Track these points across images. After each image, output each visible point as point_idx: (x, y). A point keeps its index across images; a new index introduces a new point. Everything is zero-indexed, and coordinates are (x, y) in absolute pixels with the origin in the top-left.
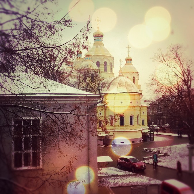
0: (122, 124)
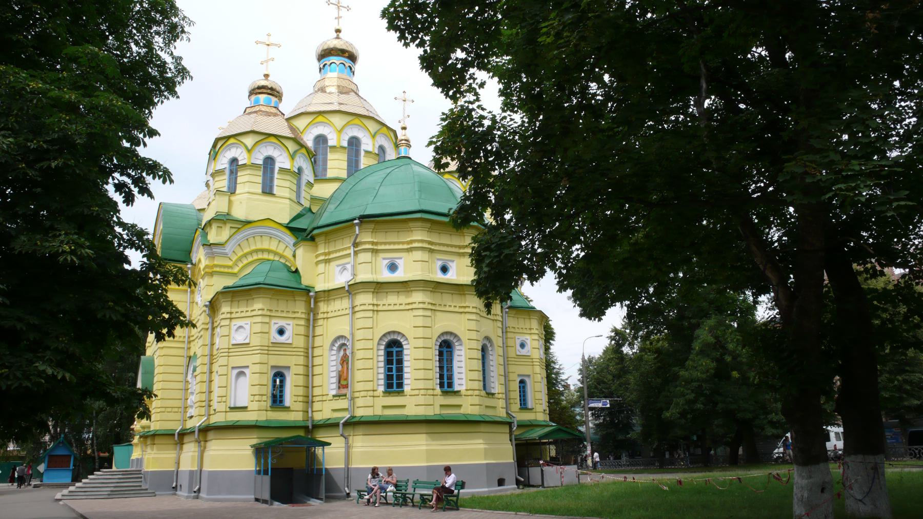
0: (394, 381)
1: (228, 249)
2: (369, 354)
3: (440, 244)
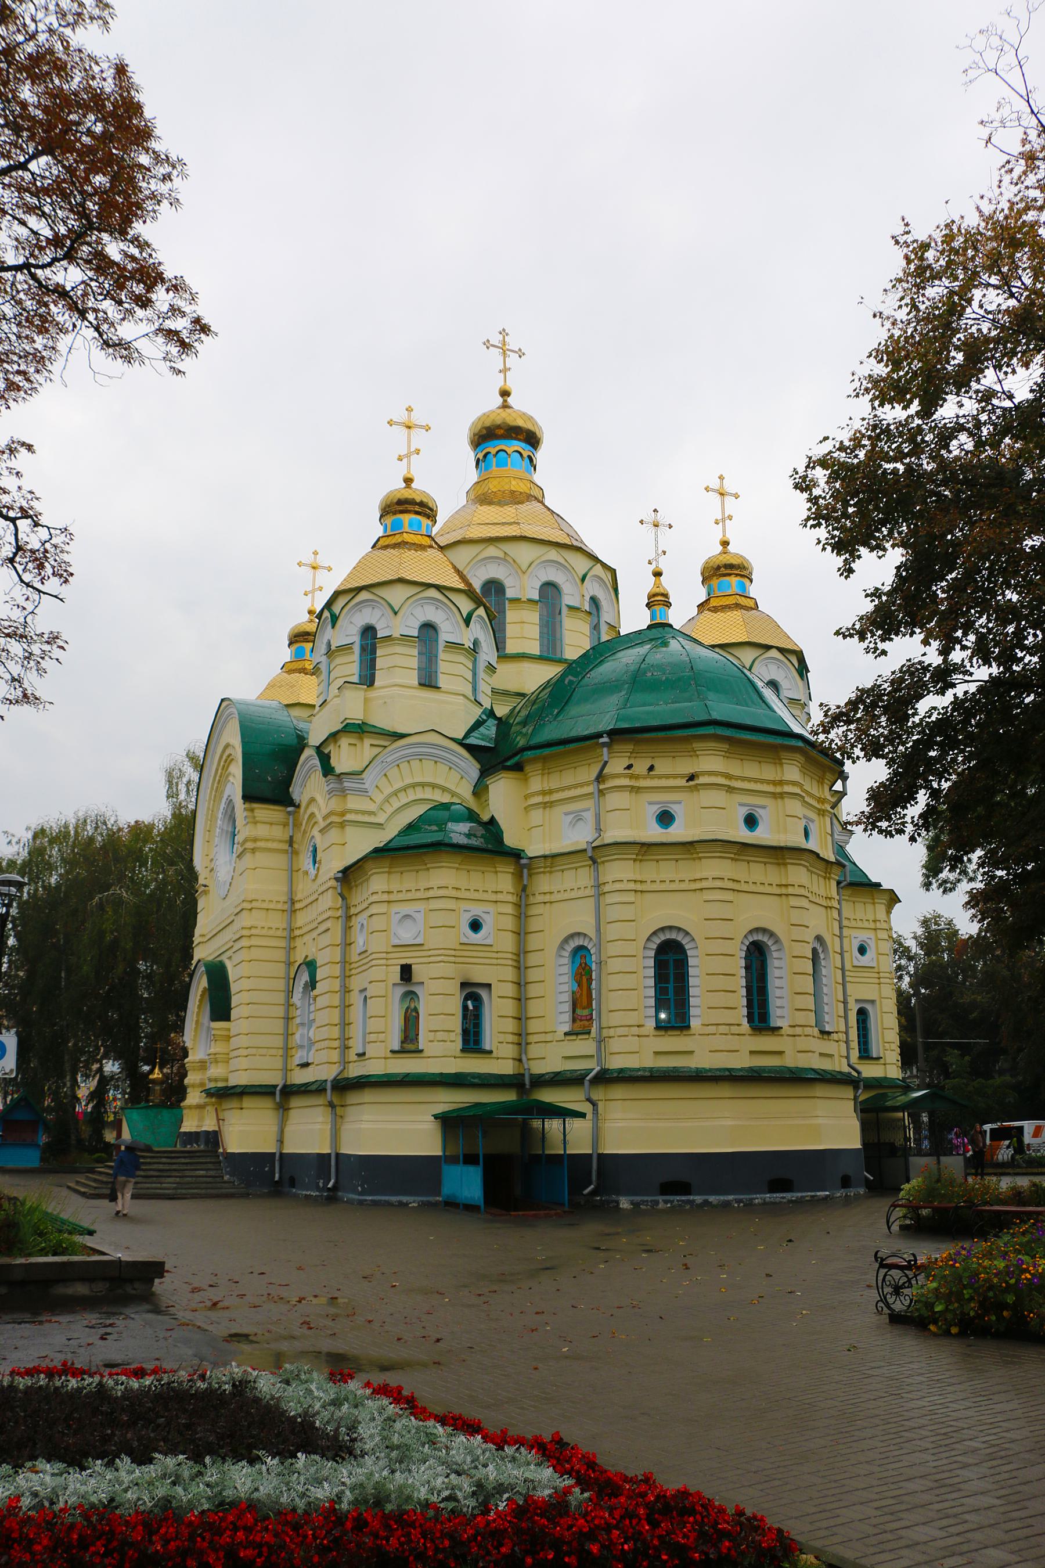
1: (369, 779)
2: (629, 965)
3: (743, 779)
